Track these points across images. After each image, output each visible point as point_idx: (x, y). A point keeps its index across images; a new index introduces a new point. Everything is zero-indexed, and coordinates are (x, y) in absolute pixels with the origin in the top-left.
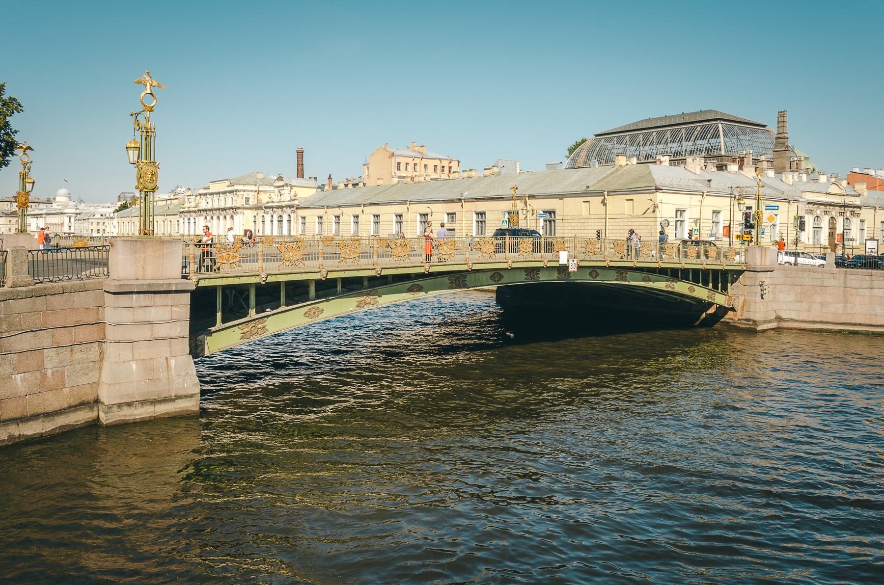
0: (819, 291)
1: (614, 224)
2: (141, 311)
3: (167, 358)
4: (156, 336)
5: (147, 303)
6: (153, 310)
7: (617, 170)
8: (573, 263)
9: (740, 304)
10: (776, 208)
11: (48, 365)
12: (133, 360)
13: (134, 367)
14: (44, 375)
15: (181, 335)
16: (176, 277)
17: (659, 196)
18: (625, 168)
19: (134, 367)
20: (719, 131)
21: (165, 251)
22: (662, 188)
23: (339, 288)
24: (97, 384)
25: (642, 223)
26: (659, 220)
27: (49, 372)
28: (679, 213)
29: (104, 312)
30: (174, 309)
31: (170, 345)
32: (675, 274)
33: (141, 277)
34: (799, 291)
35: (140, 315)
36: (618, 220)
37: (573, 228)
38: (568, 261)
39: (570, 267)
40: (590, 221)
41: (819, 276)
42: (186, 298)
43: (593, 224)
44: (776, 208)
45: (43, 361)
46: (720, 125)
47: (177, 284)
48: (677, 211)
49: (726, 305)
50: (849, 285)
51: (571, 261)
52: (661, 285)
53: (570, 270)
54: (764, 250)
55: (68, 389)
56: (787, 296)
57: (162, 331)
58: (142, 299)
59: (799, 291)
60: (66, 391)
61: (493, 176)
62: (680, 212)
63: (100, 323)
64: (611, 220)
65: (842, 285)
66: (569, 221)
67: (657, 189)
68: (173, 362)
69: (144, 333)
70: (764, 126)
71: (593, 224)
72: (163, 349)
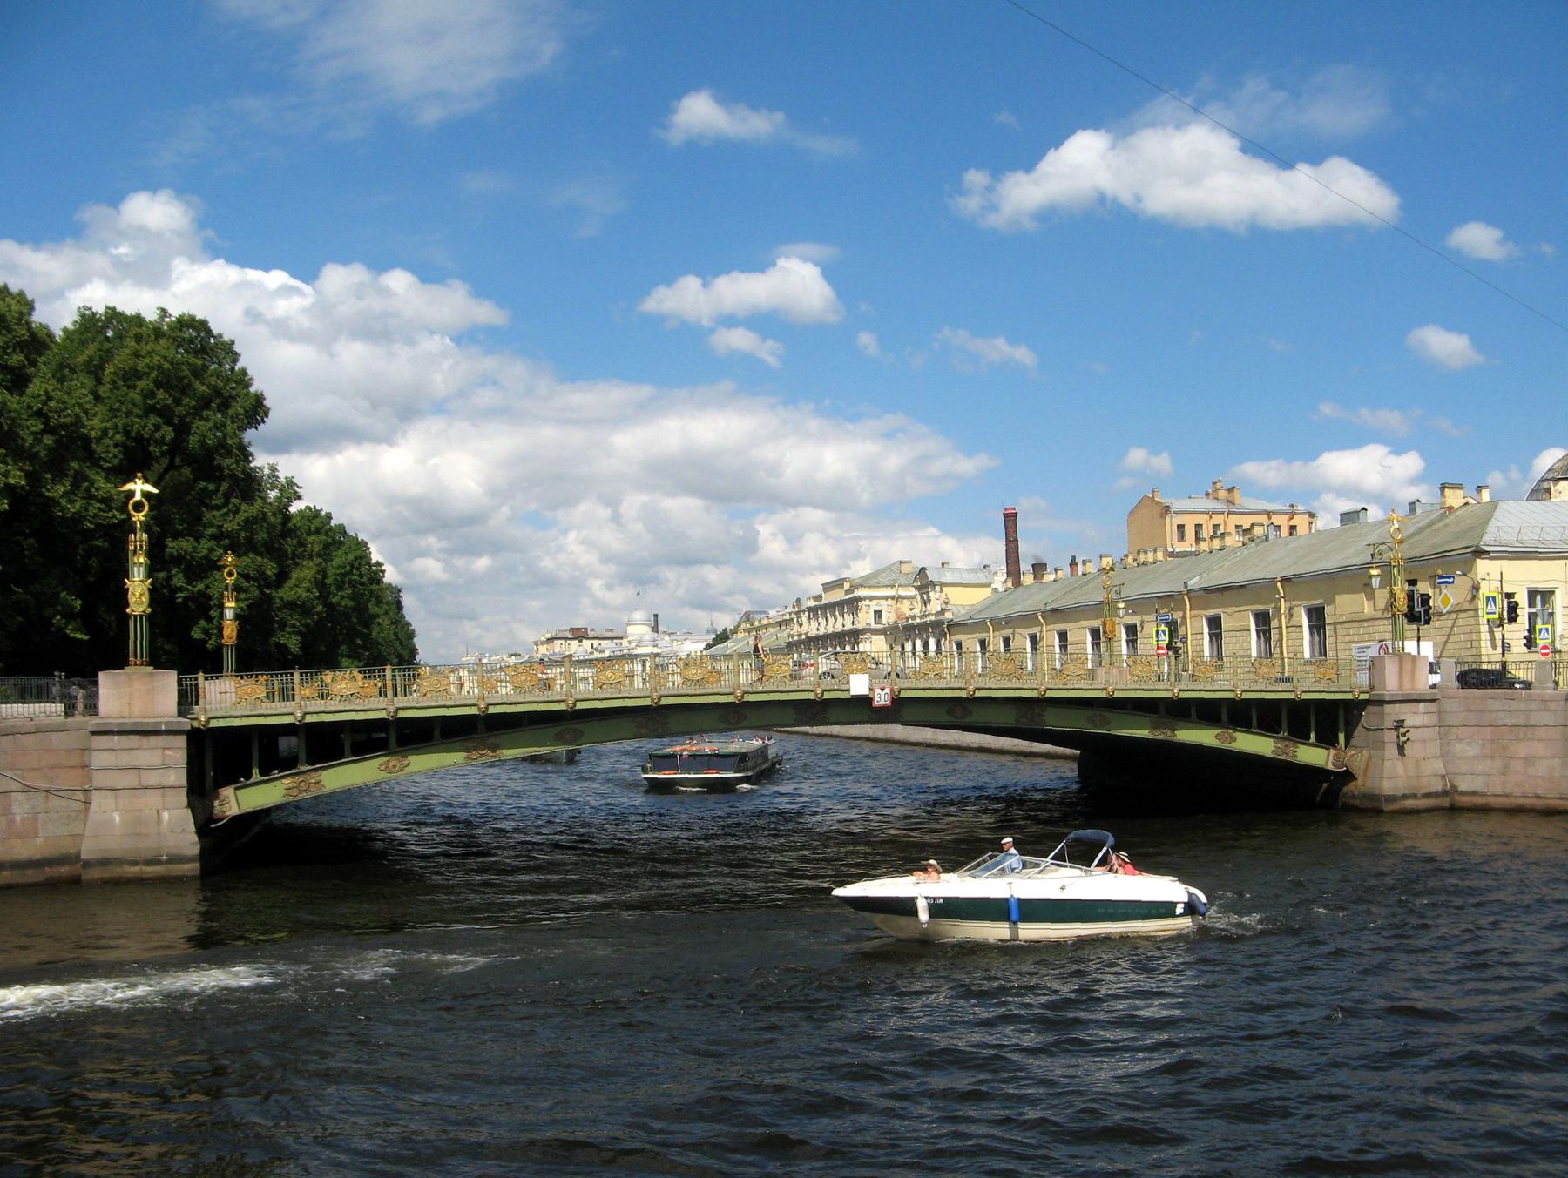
0: (1522, 736)
2: (125, 754)
3: (158, 811)
4: (145, 784)
5: (133, 745)
6: (140, 753)
8: (883, 693)
9: (1362, 767)
10: (1451, 580)
11: (16, 809)
13: (118, 819)
14: (13, 821)
15: (177, 784)
16: (170, 714)
17: (1482, 566)
18: (1458, 513)
19: (118, 819)
21: (155, 684)
22: (1487, 549)
23: (437, 733)
24: (79, 837)
27: (18, 818)
28: (1538, 598)
29: (90, 755)
30: (167, 752)
31: (164, 795)
32: (1238, 713)
33: (126, 714)
34: (1488, 737)
35: (125, 759)
37: (1351, 638)
38: (871, 690)
39: (877, 699)
40: (1376, 623)
41: (1522, 706)
42: (182, 741)
44: (1451, 580)
45: (10, 805)
47: (167, 723)
49: (1330, 767)
51: (878, 691)
52: (1205, 737)
53: (876, 703)
54: (1407, 666)
55: (42, 839)
56: (1468, 748)
57: (152, 778)
58: (134, 740)
59: (1488, 737)
60: (39, 841)
61: (1253, 544)
63: (85, 766)
66: (1346, 625)
67: (1480, 553)
68: (166, 815)
69: (129, 779)
72: (152, 800)
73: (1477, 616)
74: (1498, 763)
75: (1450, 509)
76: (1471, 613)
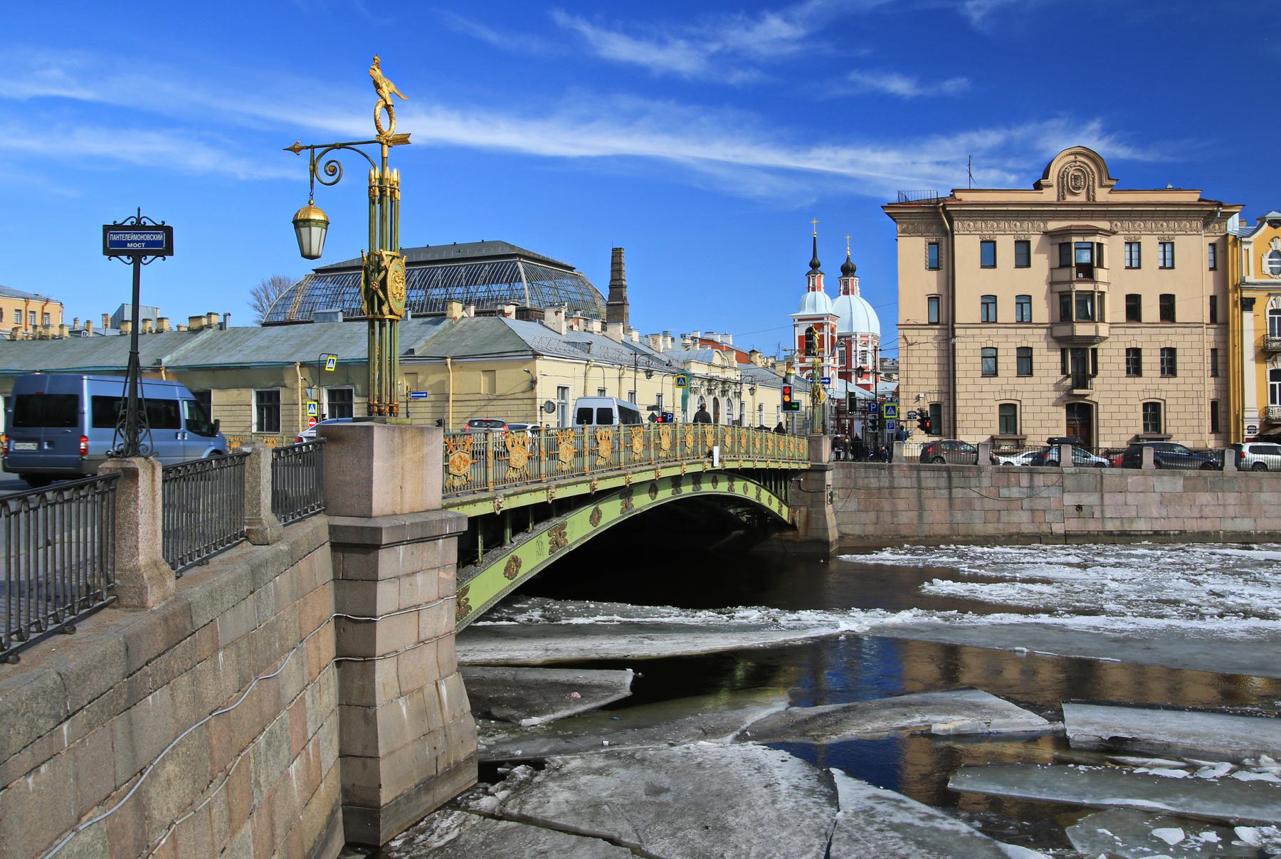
1: (462, 409)
7: (452, 326)
12: (401, 695)
18: (462, 322)
20: (519, 272)
25: (511, 408)
26: (538, 401)
36: (468, 403)
43: (423, 410)
46: (519, 264)
48: (559, 387)
50: (924, 485)
62: (563, 389)
64: (456, 404)
65: (915, 485)
67: (536, 355)
70: (572, 269)
71: (423, 410)
73: (535, 404)
74: (873, 515)
75: (455, 318)
76: (529, 402)
